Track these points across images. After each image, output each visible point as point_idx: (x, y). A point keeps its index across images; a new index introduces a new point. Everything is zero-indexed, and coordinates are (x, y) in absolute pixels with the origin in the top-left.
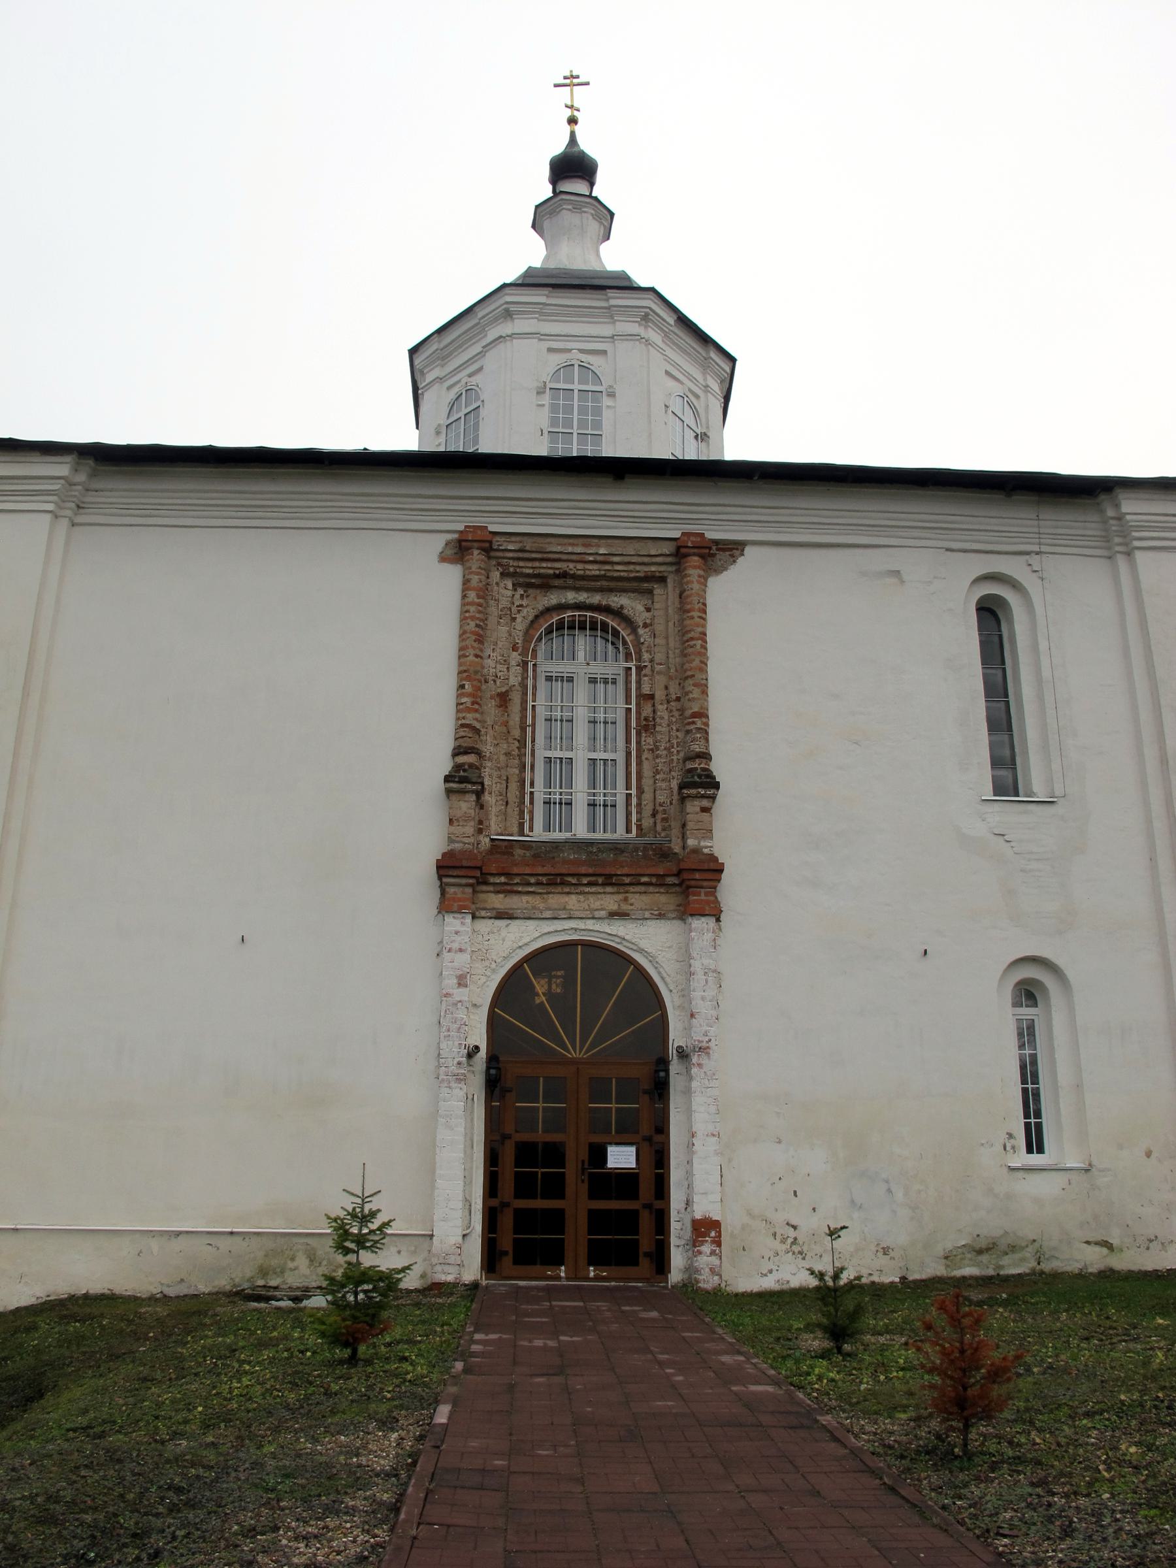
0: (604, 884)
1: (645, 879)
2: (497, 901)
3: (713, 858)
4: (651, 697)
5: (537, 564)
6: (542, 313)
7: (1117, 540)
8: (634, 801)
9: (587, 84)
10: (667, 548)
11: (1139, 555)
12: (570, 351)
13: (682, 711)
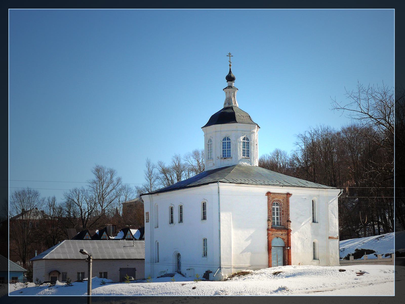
9: (233, 56)
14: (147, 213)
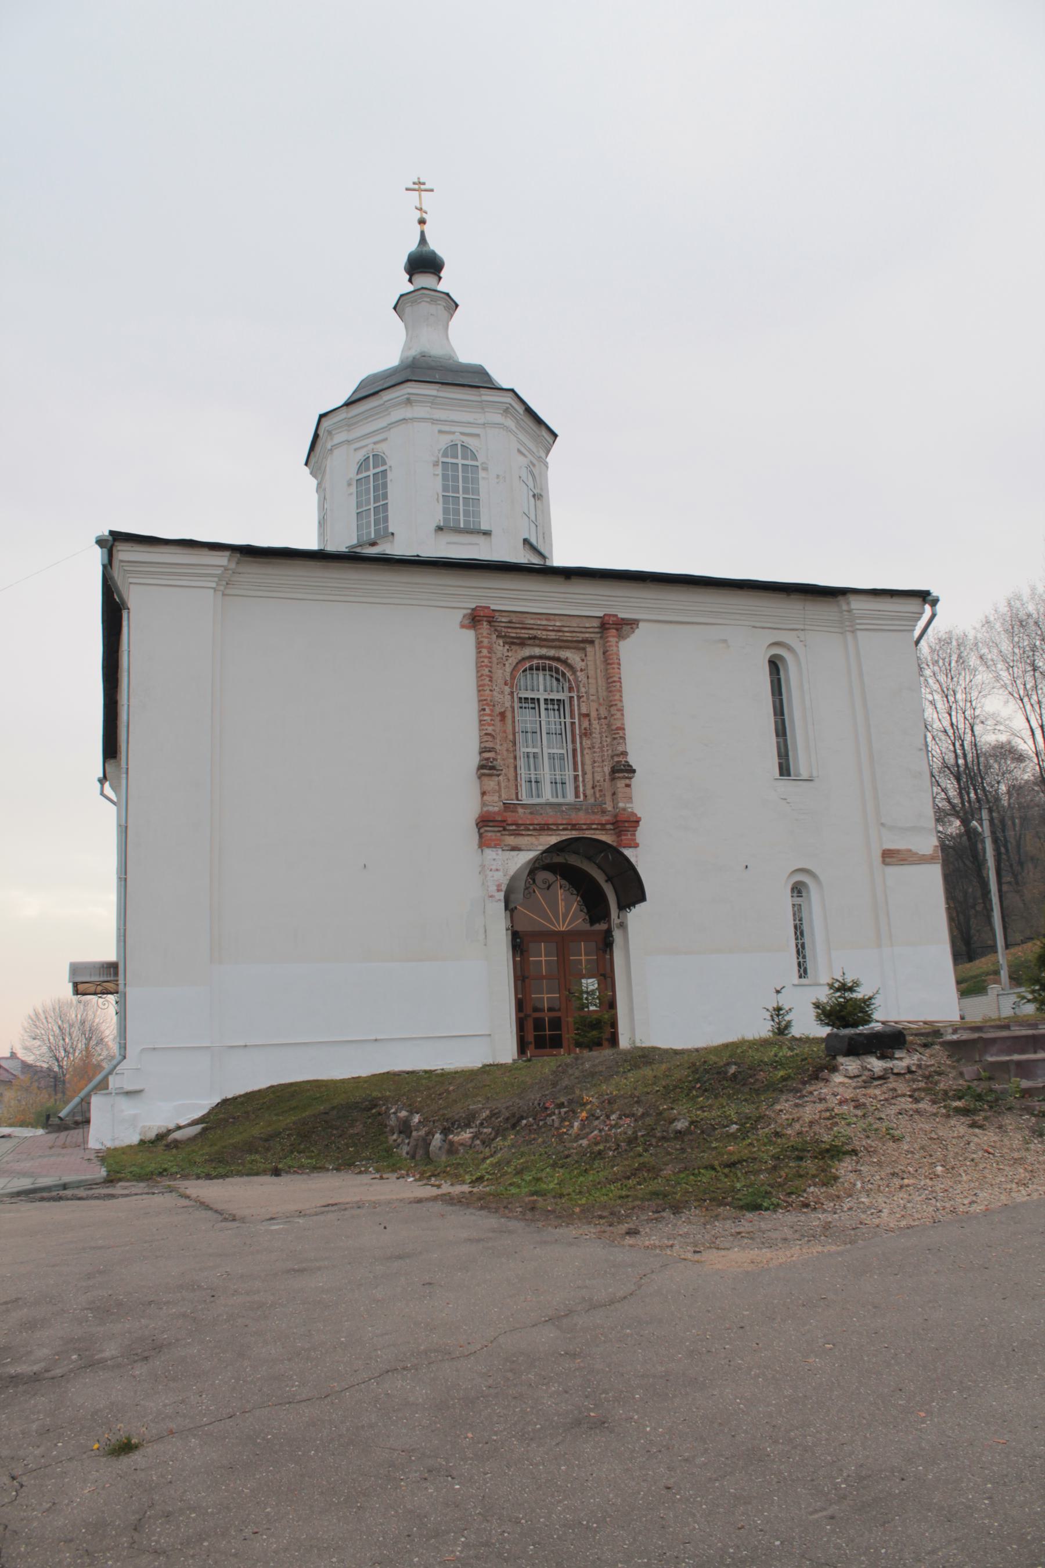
0: (572, 830)
1: (594, 826)
2: (511, 840)
3: (633, 814)
4: (588, 715)
5: (518, 631)
6: (433, 402)
7: (847, 623)
8: (581, 779)
9: (432, 190)
10: (596, 623)
11: (859, 633)
12: (454, 433)
13: (609, 725)
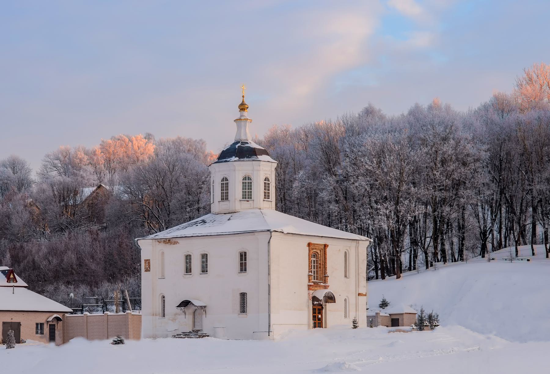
14: (148, 261)
